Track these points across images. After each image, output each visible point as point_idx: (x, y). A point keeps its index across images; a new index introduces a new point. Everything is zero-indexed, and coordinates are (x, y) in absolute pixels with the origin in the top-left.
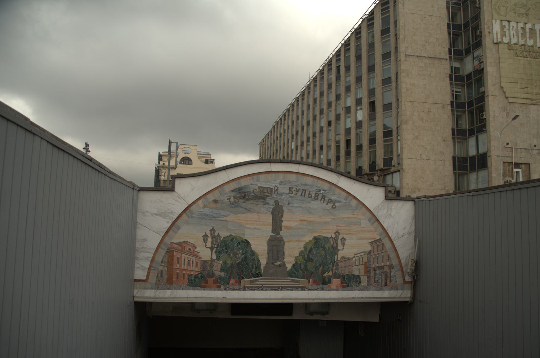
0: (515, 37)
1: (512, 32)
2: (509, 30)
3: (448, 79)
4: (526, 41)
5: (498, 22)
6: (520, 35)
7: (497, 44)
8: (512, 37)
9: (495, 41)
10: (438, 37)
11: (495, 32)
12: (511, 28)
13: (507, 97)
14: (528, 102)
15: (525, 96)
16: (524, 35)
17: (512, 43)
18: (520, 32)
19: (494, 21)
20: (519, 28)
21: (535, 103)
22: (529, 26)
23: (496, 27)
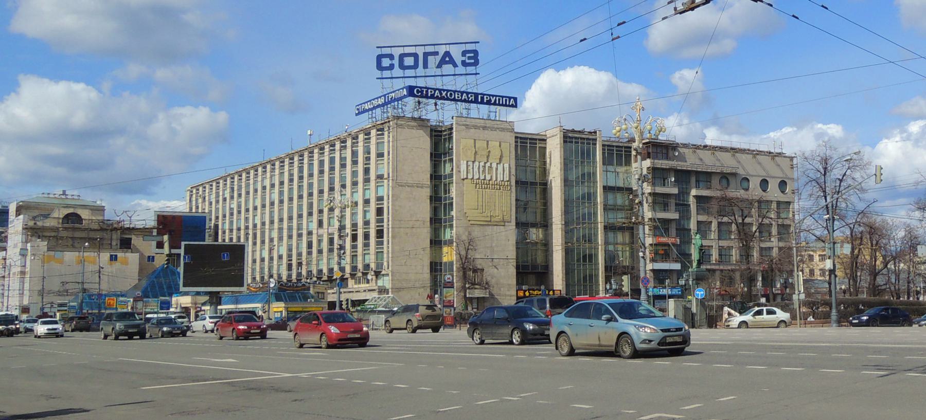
0: (478, 173)
1: (476, 169)
2: (473, 168)
3: (429, 200)
4: (485, 176)
5: (465, 162)
6: (481, 172)
7: (463, 179)
8: (475, 174)
9: (462, 178)
10: (422, 166)
11: (462, 170)
12: (475, 166)
13: (469, 221)
14: (485, 223)
15: (483, 219)
16: (484, 171)
17: (475, 178)
18: (481, 169)
19: (462, 161)
20: (481, 167)
21: (490, 223)
22: (488, 165)
23: (463, 167)
